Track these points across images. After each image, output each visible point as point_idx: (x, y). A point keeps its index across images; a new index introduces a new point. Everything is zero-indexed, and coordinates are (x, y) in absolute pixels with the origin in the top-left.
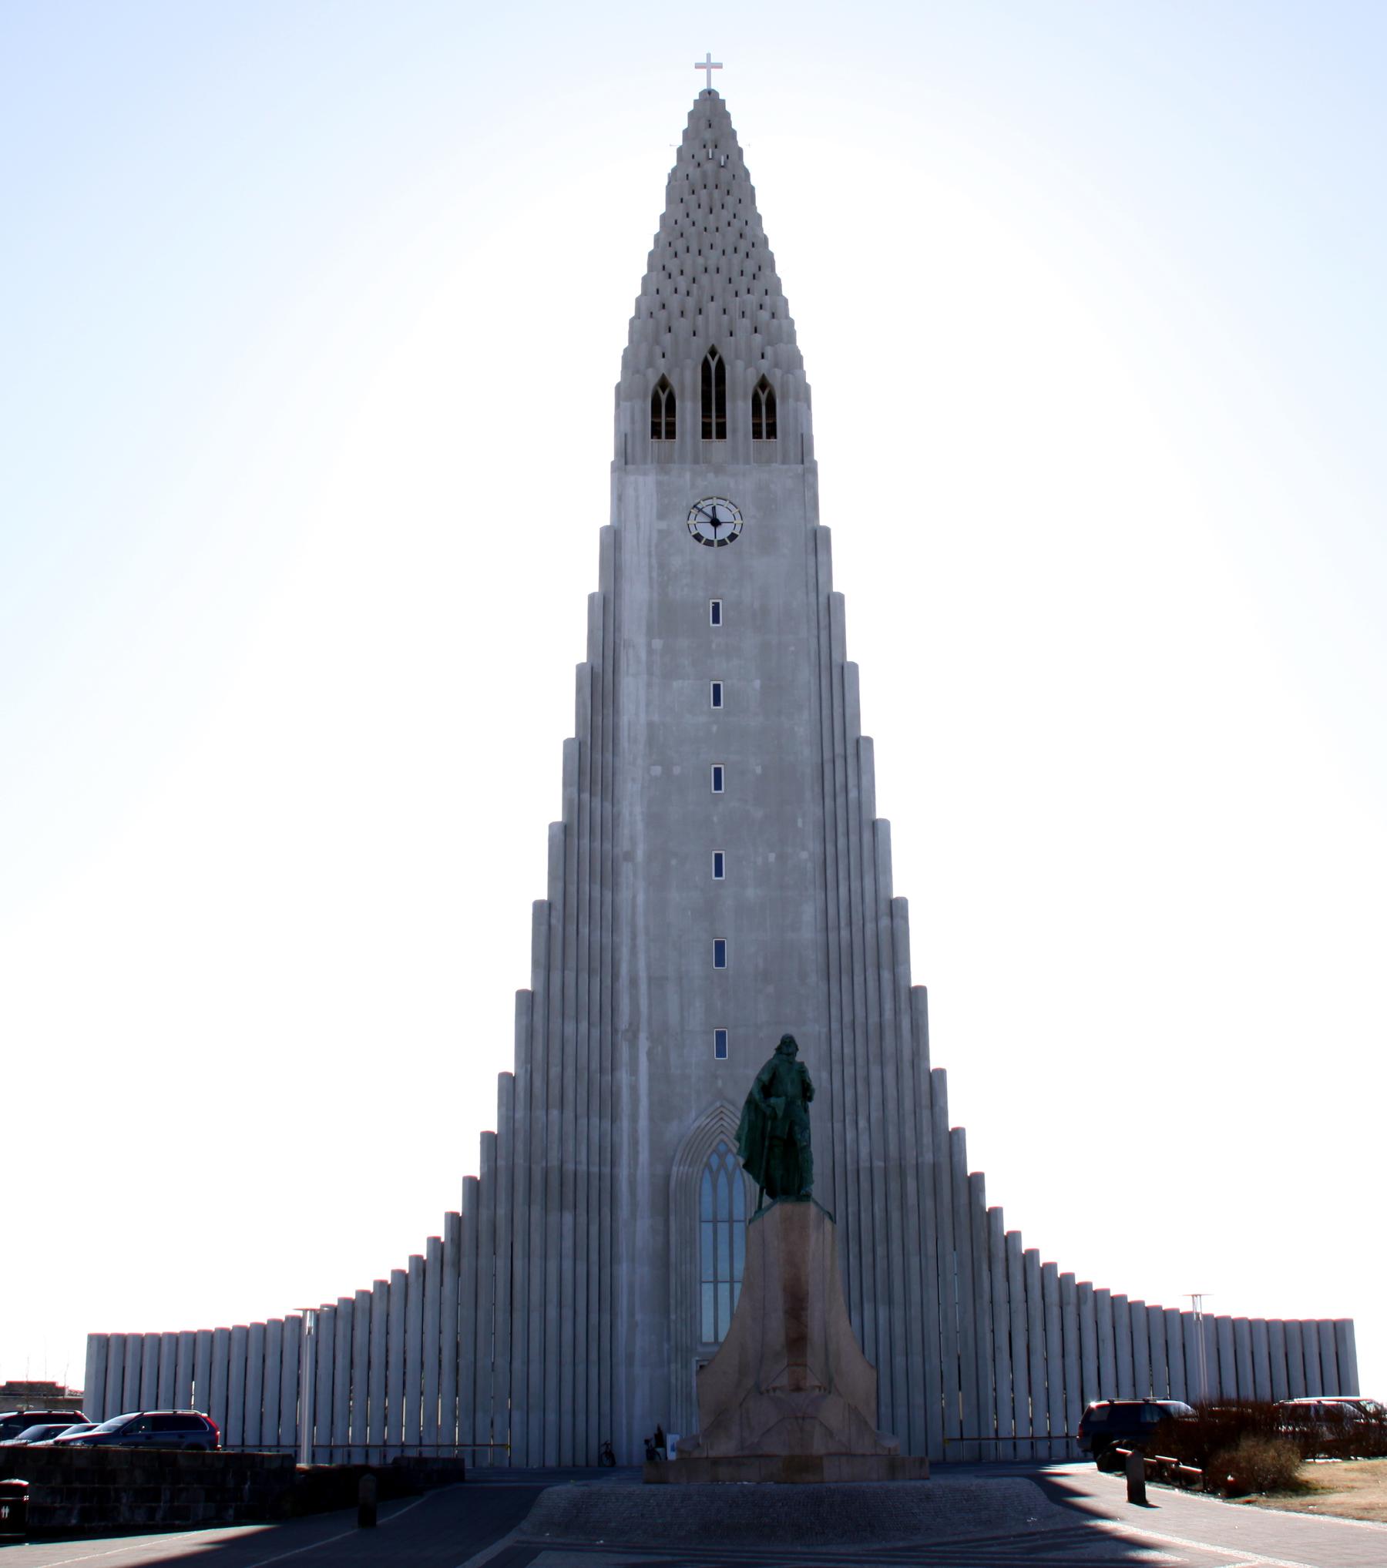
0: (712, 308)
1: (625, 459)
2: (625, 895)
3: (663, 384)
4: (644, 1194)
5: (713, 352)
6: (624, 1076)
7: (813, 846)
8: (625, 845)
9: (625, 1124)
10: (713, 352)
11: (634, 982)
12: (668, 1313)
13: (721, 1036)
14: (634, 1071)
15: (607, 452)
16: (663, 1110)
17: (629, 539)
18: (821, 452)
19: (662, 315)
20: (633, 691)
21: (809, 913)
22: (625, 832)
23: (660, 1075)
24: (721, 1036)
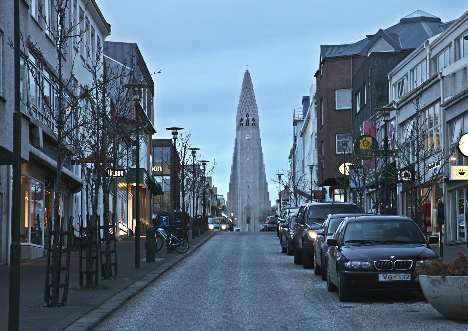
0: (247, 108)
1: (238, 129)
2: (238, 181)
3: (242, 120)
4: (240, 212)
5: (248, 114)
6: (238, 201)
7: (258, 175)
8: (238, 175)
9: (238, 205)
10: (248, 114)
11: (239, 190)
12: (242, 224)
13: (248, 196)
14: (239, 199)
15: (235, 128)
16: (243, 204)
17: (238, 139)
18: (260, 128)
19: (241, 109)
20: (239, 157)
21: (258, 183)
22: (238, 174)
23: (242, 200)
24: (248, 196)
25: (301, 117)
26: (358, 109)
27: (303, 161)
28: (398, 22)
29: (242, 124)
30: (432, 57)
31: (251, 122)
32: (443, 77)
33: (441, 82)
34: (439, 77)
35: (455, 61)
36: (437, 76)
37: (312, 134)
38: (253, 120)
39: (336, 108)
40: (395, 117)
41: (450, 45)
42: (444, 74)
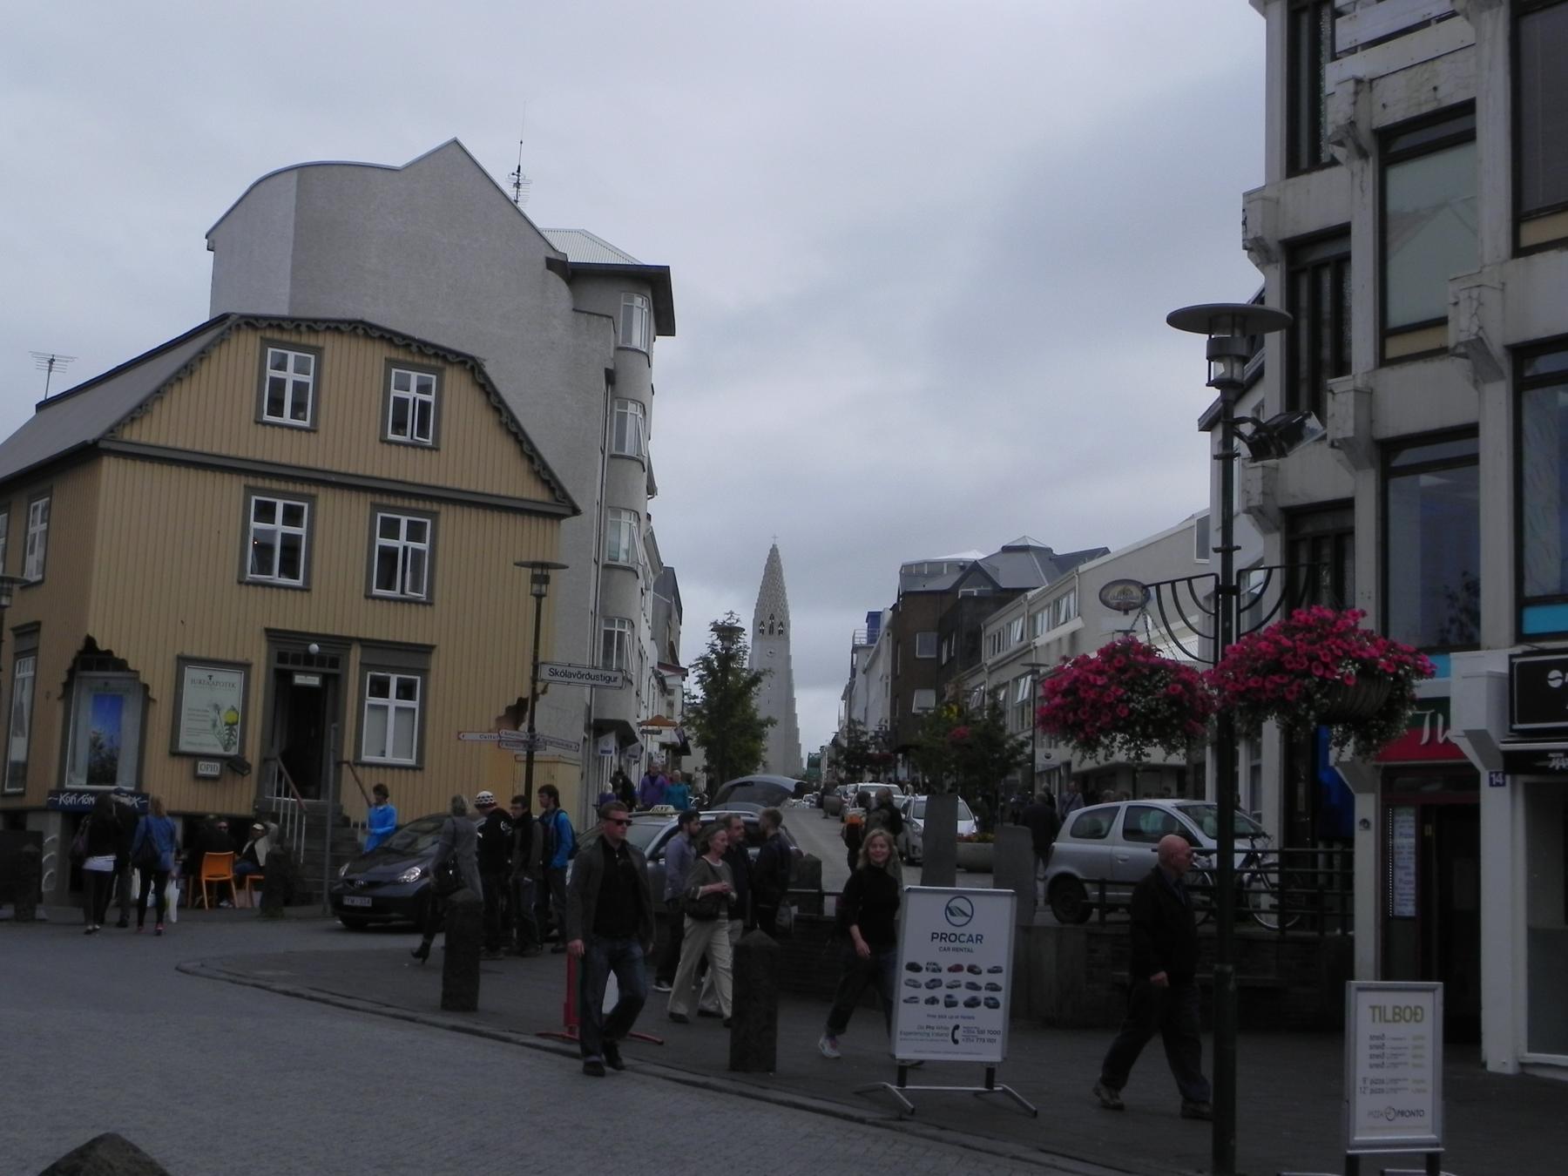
0: (773, 605)
3: (762, 623)
25: (864, 642)
26: (944, 659)
27: (866, 710)
28: (999, 549)
29: (762, 631)
30: (1030, 613)
31: (777, 629)
32: (1036, 648)
33: (1034, 653)
34: (1032, 647)
35: (1048, 630)
36: (1030, 645)
37: (882, 677)
38: (781, 624)
39: (917, 655)
40: (985, 682)
41: (1048, 606)
42: (1037, 645)
